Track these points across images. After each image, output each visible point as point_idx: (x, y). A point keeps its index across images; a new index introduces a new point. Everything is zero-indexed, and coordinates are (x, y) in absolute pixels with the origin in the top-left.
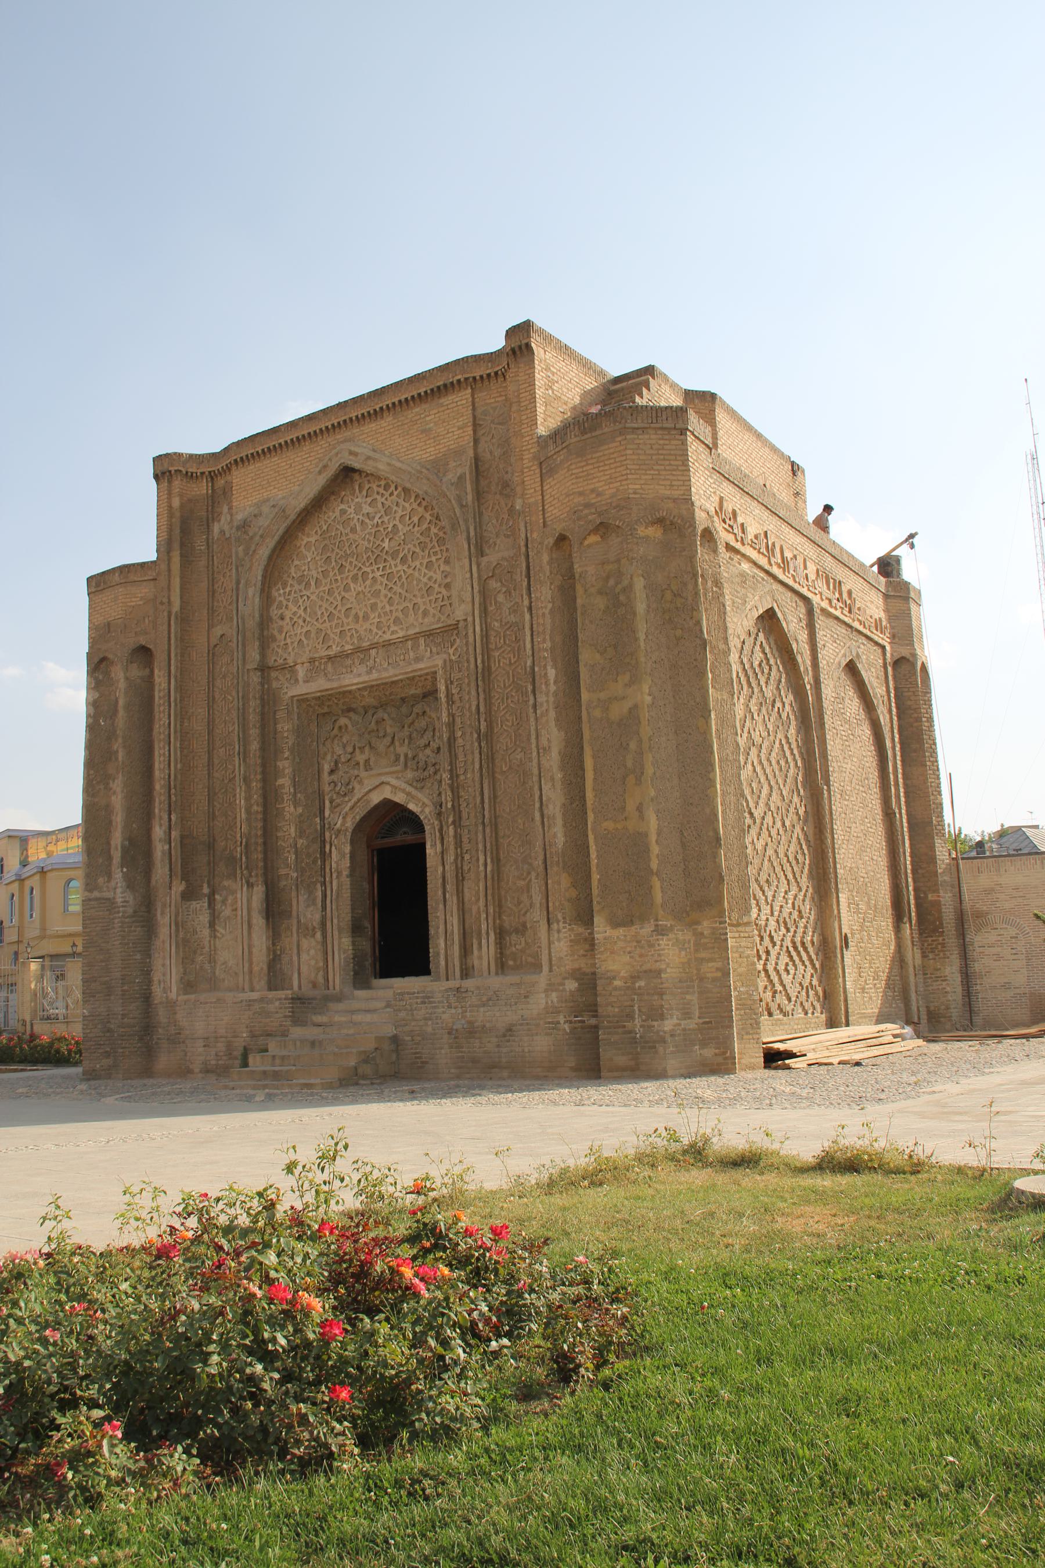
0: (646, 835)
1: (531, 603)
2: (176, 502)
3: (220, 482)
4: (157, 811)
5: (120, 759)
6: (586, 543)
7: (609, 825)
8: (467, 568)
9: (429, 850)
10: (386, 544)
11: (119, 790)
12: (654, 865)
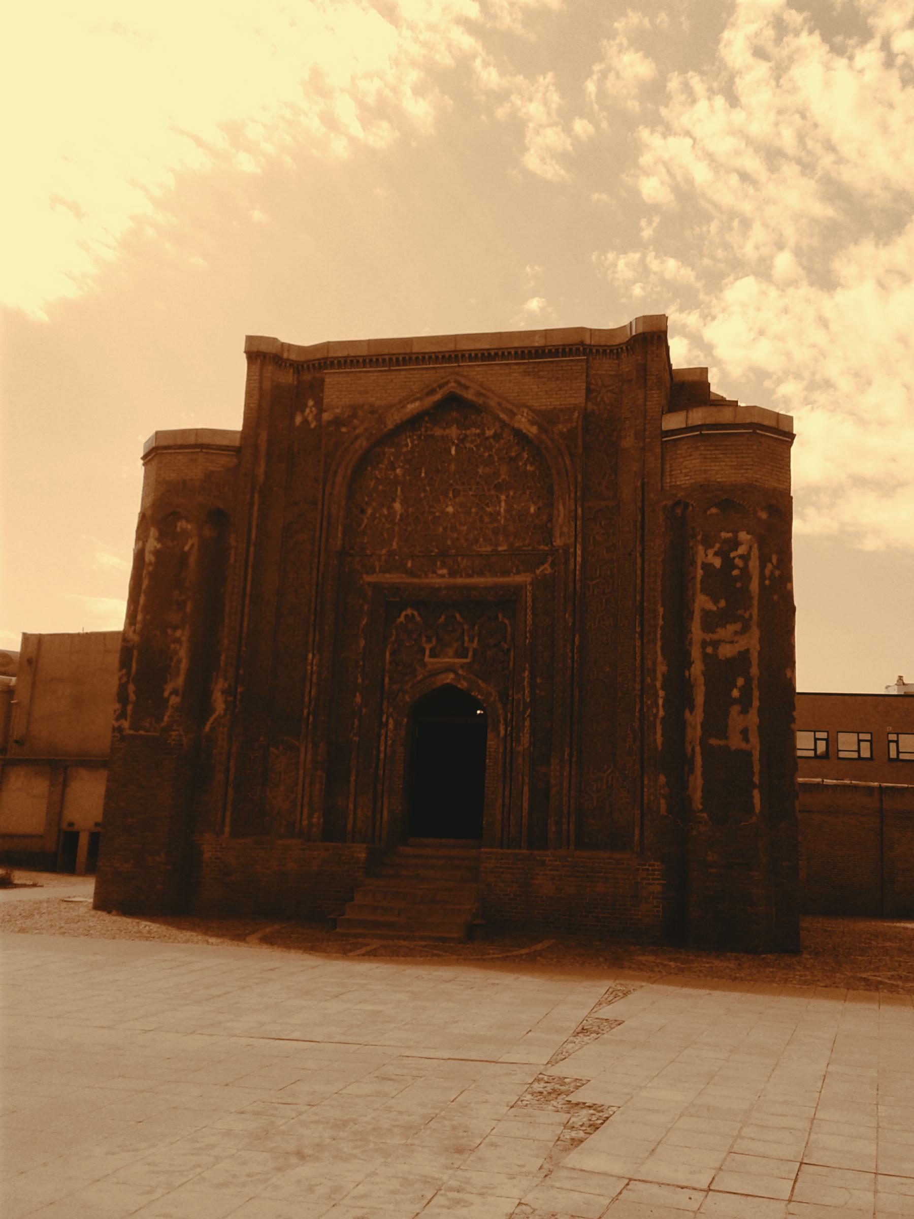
0: (750, 754)
1: (643, 550)
2: (267, 385)
3: (307, 377)
4: (222, 664)
5: (188, 609)
6: (708, 513)
7: (713, 742)
8: (573, 508)
9: (490, 736)
10: (480, 470)
11: (184, 639)
12: (756, 779)
